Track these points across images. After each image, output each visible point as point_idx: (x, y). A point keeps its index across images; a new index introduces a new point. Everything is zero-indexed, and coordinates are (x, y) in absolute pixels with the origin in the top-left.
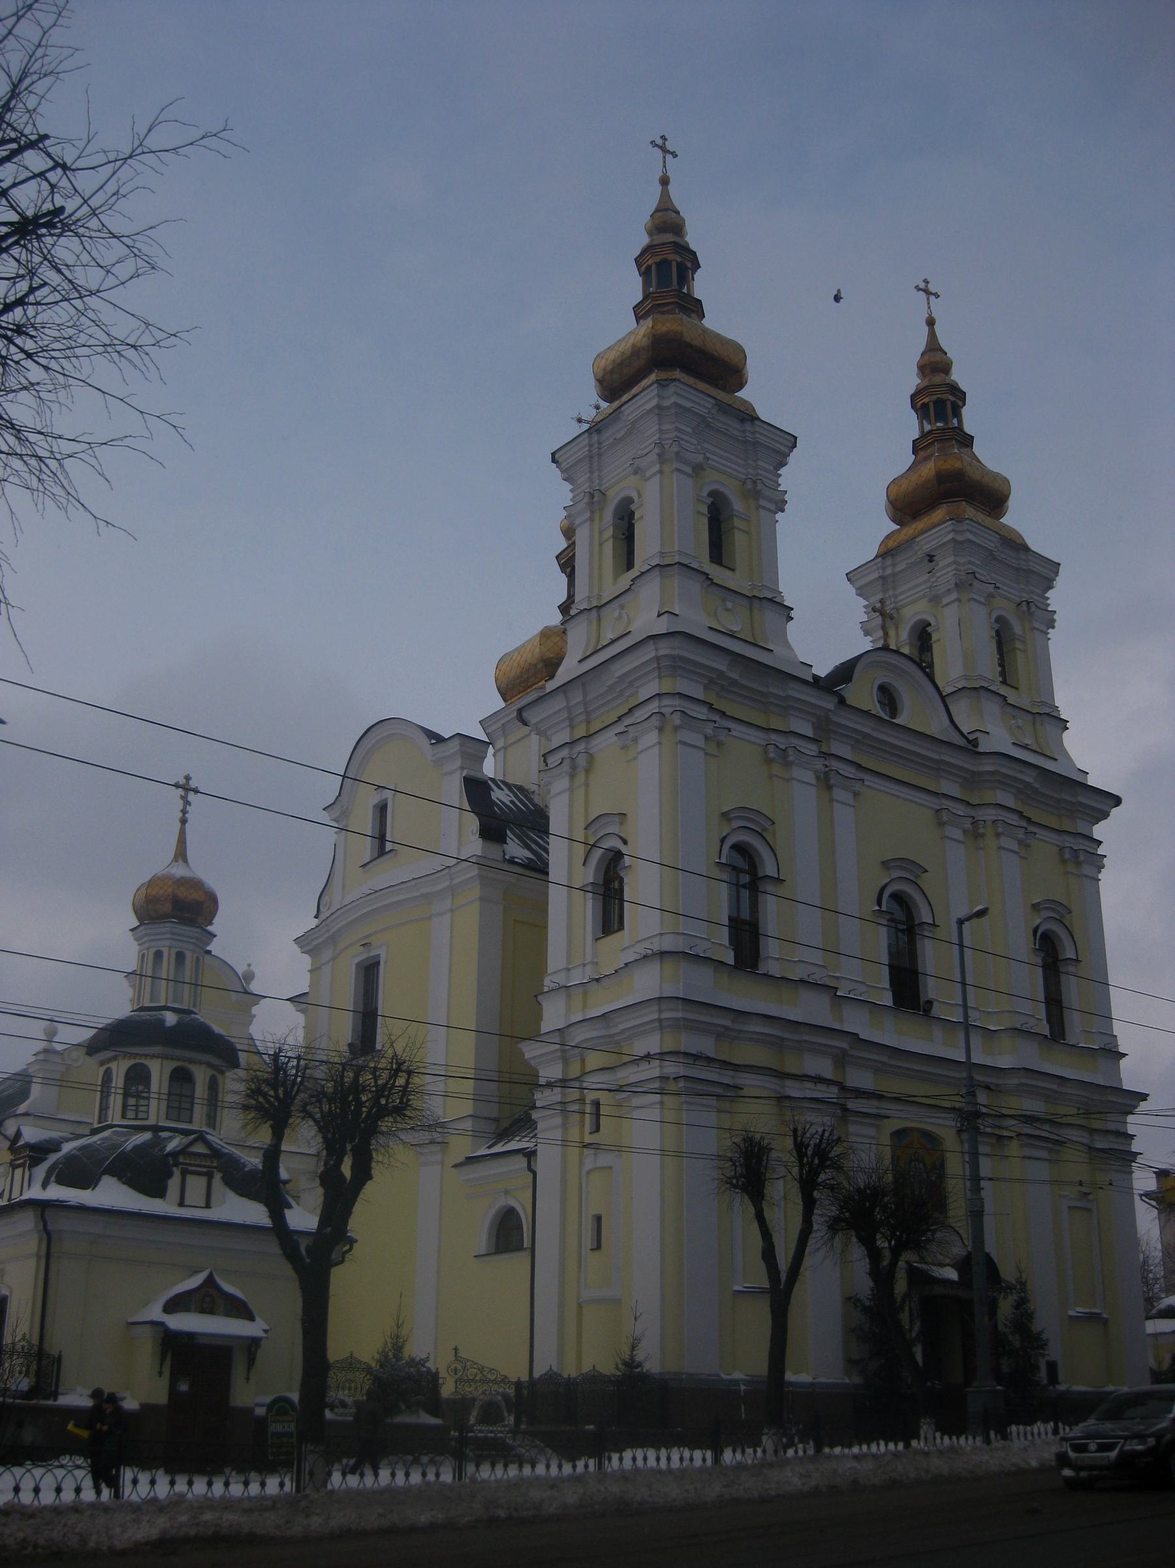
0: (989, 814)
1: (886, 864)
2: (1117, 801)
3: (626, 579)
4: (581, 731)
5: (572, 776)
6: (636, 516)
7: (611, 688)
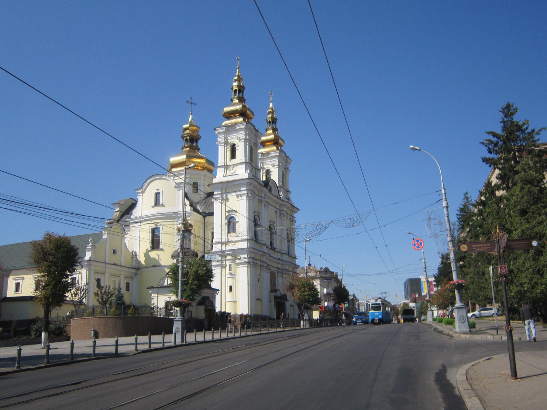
0: (283, 212)
1: (270, 221)
2: (299, 210)
3: (234, 162)
6: (237, 148)
7: (234, 185)
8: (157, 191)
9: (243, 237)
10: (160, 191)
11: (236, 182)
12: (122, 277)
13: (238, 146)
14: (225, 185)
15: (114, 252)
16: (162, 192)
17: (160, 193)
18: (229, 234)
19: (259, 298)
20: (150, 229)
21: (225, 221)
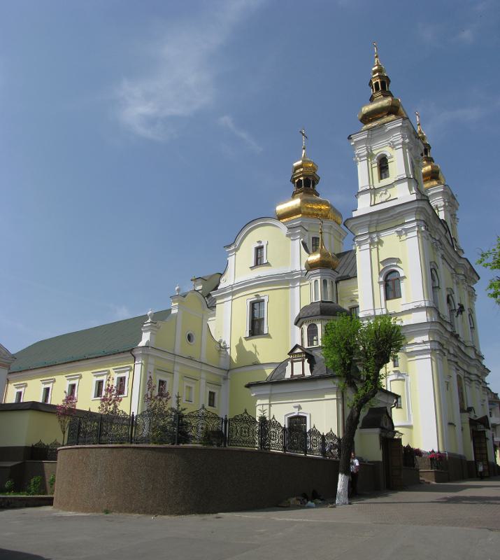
3: (385, 182)
4: (373, 229)
5: (371, 244)
7: (392, 216)
8: (258, 245)
9: (418, 304)
10: (264, 244)
11: (396, 209)
12: (203, 382)
13: (392, 157)
14: (376, 217)
15: (190, 338)
16: (267, 244)
17: (262, 247)
18: (388, 302)
19: (452, 421)
20: (248, 303)
21: (378, 279)
